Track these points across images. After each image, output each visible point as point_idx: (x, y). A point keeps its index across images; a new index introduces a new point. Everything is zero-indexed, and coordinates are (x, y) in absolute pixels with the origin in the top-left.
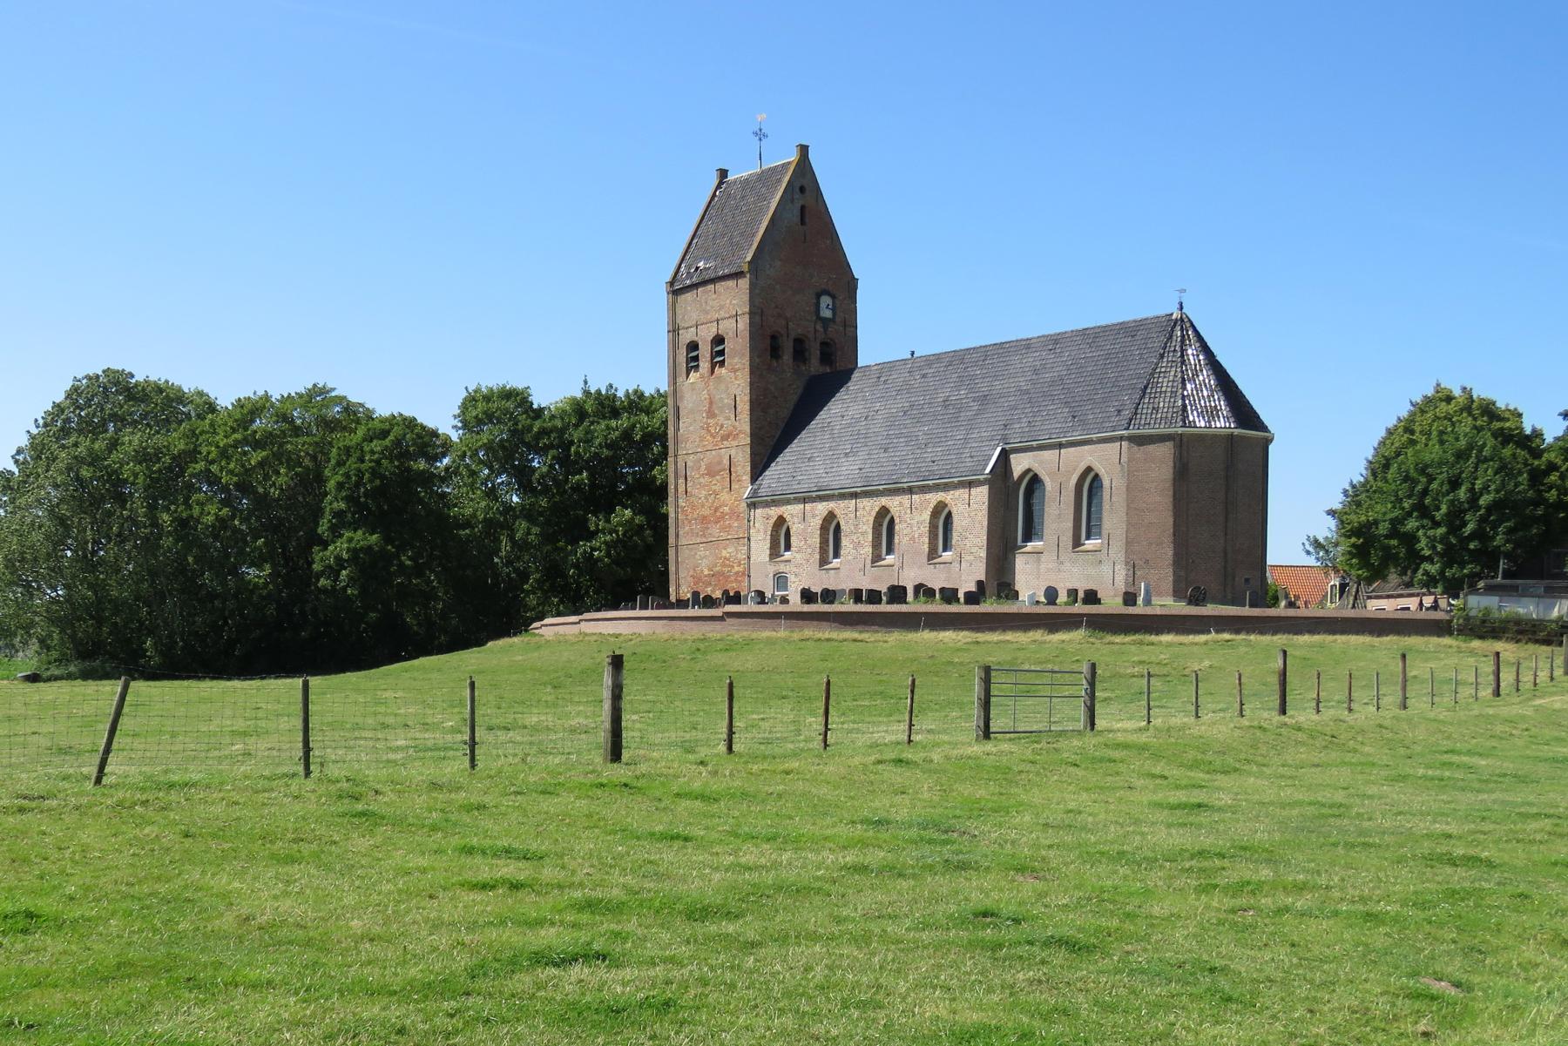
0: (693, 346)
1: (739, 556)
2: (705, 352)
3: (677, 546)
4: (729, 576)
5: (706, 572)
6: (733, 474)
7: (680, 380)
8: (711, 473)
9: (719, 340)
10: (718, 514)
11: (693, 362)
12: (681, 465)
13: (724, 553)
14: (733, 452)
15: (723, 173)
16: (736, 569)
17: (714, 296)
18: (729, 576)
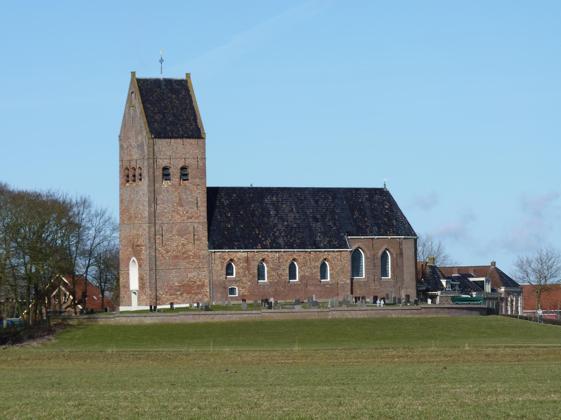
0: (165, 169)
1: (200, 276)
2: (175, 172)
3: (156, 270)
4: (193, 287)
5: (177, 284)
6: (196, 237)
7: (157, 185)
8: (181, 233)
9: (184, 168)
10: (185, 256)
11: (166, 175)
12: (157, 227)
13: (190, 275)
14: (196, 225)
15: (133, 74)
16: (199, 283)
17: (182, 146)
18: (193, 287)
